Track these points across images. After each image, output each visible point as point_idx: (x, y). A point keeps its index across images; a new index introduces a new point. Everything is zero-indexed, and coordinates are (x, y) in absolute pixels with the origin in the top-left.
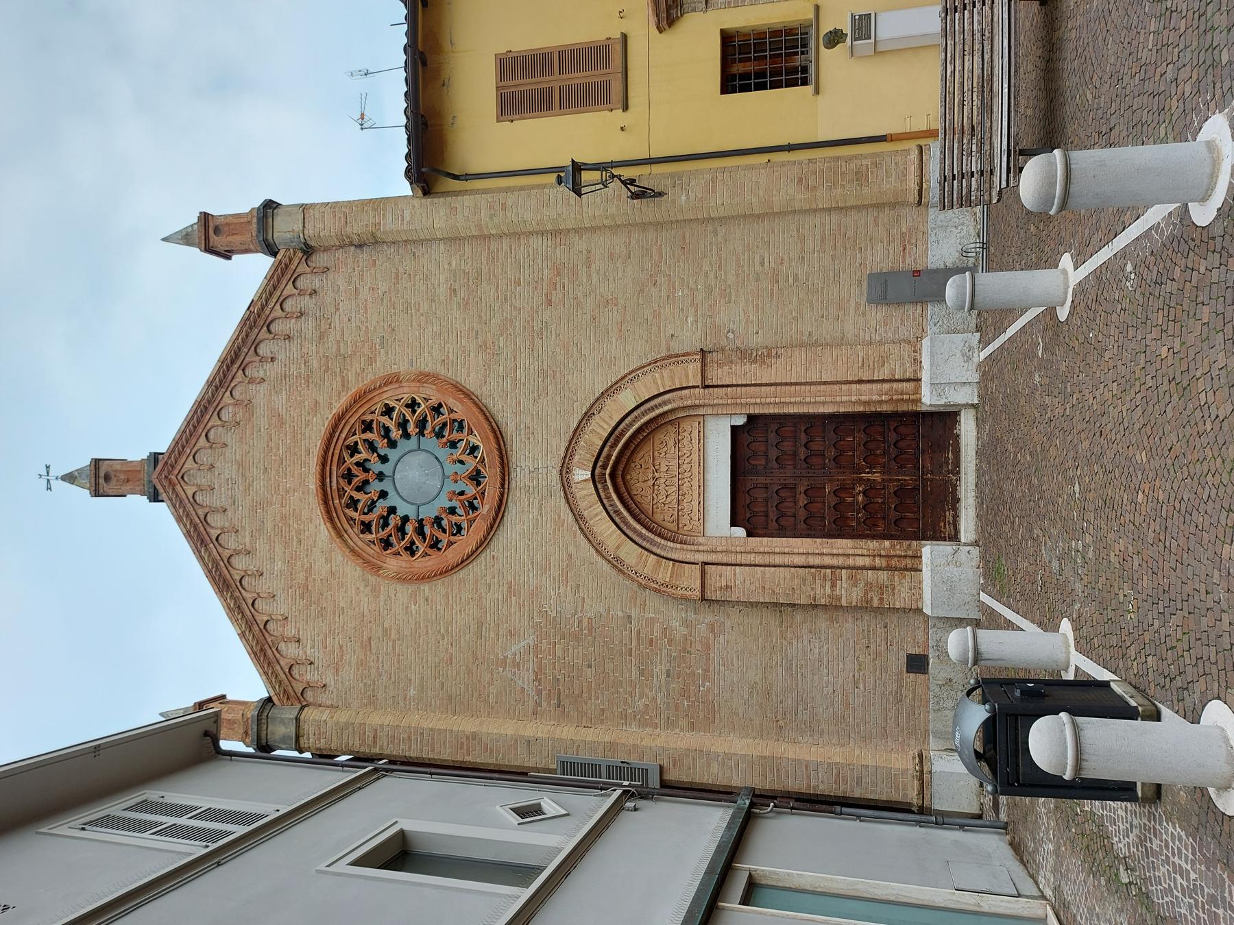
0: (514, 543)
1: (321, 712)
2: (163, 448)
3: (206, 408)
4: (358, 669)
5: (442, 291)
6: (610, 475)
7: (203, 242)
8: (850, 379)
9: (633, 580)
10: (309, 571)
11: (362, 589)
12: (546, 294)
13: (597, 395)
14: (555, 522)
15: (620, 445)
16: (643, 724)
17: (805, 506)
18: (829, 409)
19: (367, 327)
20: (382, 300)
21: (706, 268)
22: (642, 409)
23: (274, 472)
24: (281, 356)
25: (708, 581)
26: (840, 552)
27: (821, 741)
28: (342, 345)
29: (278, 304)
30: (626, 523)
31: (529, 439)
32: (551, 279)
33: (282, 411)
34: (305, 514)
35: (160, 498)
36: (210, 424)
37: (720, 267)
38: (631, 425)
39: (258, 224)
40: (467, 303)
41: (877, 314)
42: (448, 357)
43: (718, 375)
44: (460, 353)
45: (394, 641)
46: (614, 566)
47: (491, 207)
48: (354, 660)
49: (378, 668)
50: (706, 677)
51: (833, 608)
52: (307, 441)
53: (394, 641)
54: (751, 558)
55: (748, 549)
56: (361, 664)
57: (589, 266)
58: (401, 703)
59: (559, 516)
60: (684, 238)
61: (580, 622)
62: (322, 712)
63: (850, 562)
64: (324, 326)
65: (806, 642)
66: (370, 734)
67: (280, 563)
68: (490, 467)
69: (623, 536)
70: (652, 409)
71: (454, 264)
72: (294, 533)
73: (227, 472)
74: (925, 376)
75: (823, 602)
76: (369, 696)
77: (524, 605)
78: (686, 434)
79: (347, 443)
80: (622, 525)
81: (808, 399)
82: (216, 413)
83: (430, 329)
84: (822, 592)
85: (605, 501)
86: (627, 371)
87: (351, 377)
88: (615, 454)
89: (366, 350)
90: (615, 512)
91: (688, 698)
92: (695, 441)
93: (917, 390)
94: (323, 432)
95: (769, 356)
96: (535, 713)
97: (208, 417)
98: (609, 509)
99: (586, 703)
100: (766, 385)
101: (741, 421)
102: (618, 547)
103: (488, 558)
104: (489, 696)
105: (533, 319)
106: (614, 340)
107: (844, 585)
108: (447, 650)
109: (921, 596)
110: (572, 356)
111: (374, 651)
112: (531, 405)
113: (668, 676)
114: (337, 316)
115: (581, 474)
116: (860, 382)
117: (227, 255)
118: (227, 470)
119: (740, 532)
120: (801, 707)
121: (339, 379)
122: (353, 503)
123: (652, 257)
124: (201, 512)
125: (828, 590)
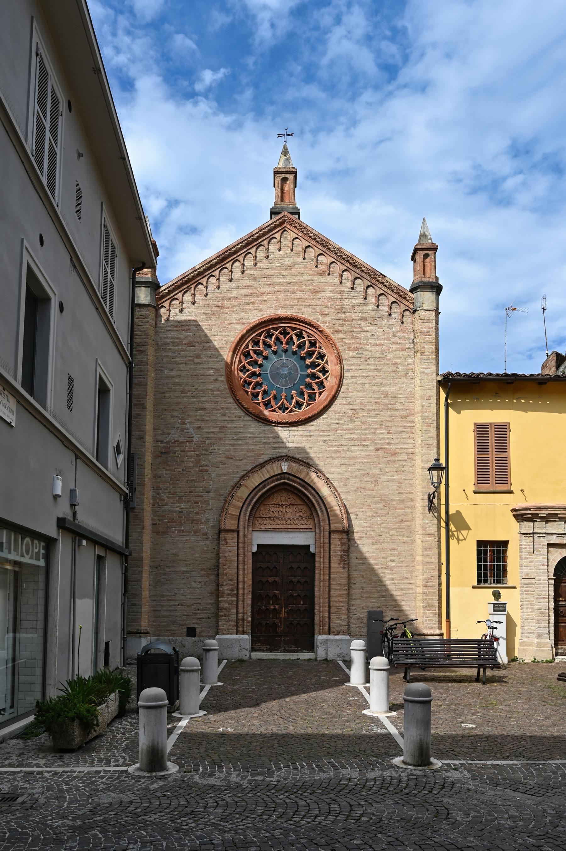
0: (248, 429)
1: (153, 319)
2: (304, 218)
3: (325, 246)
4: (177, 339)
5: (386, 389)
6: (285, 483)
7: (420, 247)
8: (331, 602)
9: (229, 494)
10: (232, 310)
11: (222, 341)
12: (382, 448)
13: (327, 475)
14: (259, 451)
15: (301, 488)
16: (154, 498)
17: (268, 581)
18: (317, 593)
19: (368, 345)
20: (383, 355)
21: (391, 533)
22: (319, 500)
23: (288, 288)
24: (353, 293)
25: (229, 533)
26: (245, 597)
27: (151, 587)
28: (359, 330)
29: (383, 292)
30: (259, 491)
31: (305, 437)
32: (390, 450)
33: (322, 294)
34: (264, 307)
35: (273, 216)
36: (316, 248)
37: (391, 539)
38: (311, 494)
39: (429, 282)
40: (379, 404)
41: (363, 615)
42: (351, 392)
43: (335, 539)
44: (352, 399)
45: (193, 361)
46: (236, 484)
47: (429, 419)
48: (183, 337)
49: (178, 351)
50: (180, 531)
51: (217, 594)
52: (305, 309)
53: (193, 361)
54: (241, 555)
55: (246, 553)
56: (181, 341)
57: (395, 471)
58: (159, 365)
59: (263, 454)
60: (407, 521)
61: (206, 466)
62: (153, 319)
63: (240, 602)
64: (370, 320)
65: (200, 580)
66: (142, 348)
67: (236, 292)
68: (289, 416)
69: (252, 489)
70: (319, 505)
71: (401, 396)
72: (253, 300)
73: (288, 259)
74: (331, 637)
75: (220, 589)
76: (162, 346)
77: (214, 434)
78: (306, 522)
79: (304, 333)
80: (258, 488)
81: (322, 583)
82: (322, 252)
83: (366, 382)
84: (226, 589)
85: (271, 480)
86: (339, 491)
87: (341, 336)
88: (295, 485)
89: (355, 345)
90: (265, 485)
91: (168, 522)
92: (302, 527)
93: (324, 634)
94: (309, 318)
95: (344, 564)
96: (157, 441)
97: (320, 247)
98: (267, 482)
99: (164, 468)
100: (330, 563)
101: (312, 550)
102: (246, 487)
103: (240, 414)
104: (165, 415)
105: (369, 440)
106: (356, 484)
107: (229, 599)
108: (189, 391)
109: (224, 634)
110: (349, 462)
111: (188, 349)
112: (322, 439)
113: (180, 512)
114: (375, 328)
115: (285, 467)
116: (329, 607)
117: (413, 258)
118: (289, 258)
119: (255, 549)
120: (167, 578)
121: (340, 328)
122: (270, 336)
123: (399, 505)
124: (265, 243)
125: (226, 592)
